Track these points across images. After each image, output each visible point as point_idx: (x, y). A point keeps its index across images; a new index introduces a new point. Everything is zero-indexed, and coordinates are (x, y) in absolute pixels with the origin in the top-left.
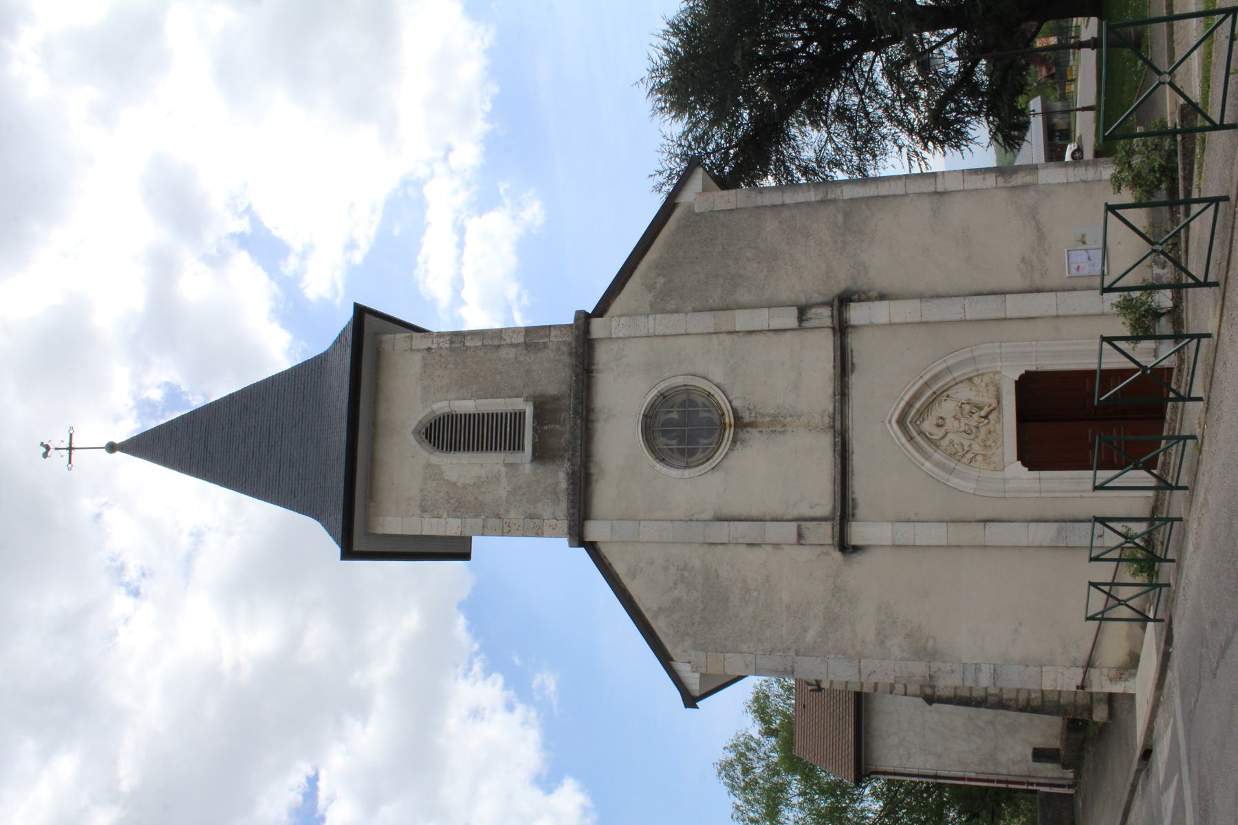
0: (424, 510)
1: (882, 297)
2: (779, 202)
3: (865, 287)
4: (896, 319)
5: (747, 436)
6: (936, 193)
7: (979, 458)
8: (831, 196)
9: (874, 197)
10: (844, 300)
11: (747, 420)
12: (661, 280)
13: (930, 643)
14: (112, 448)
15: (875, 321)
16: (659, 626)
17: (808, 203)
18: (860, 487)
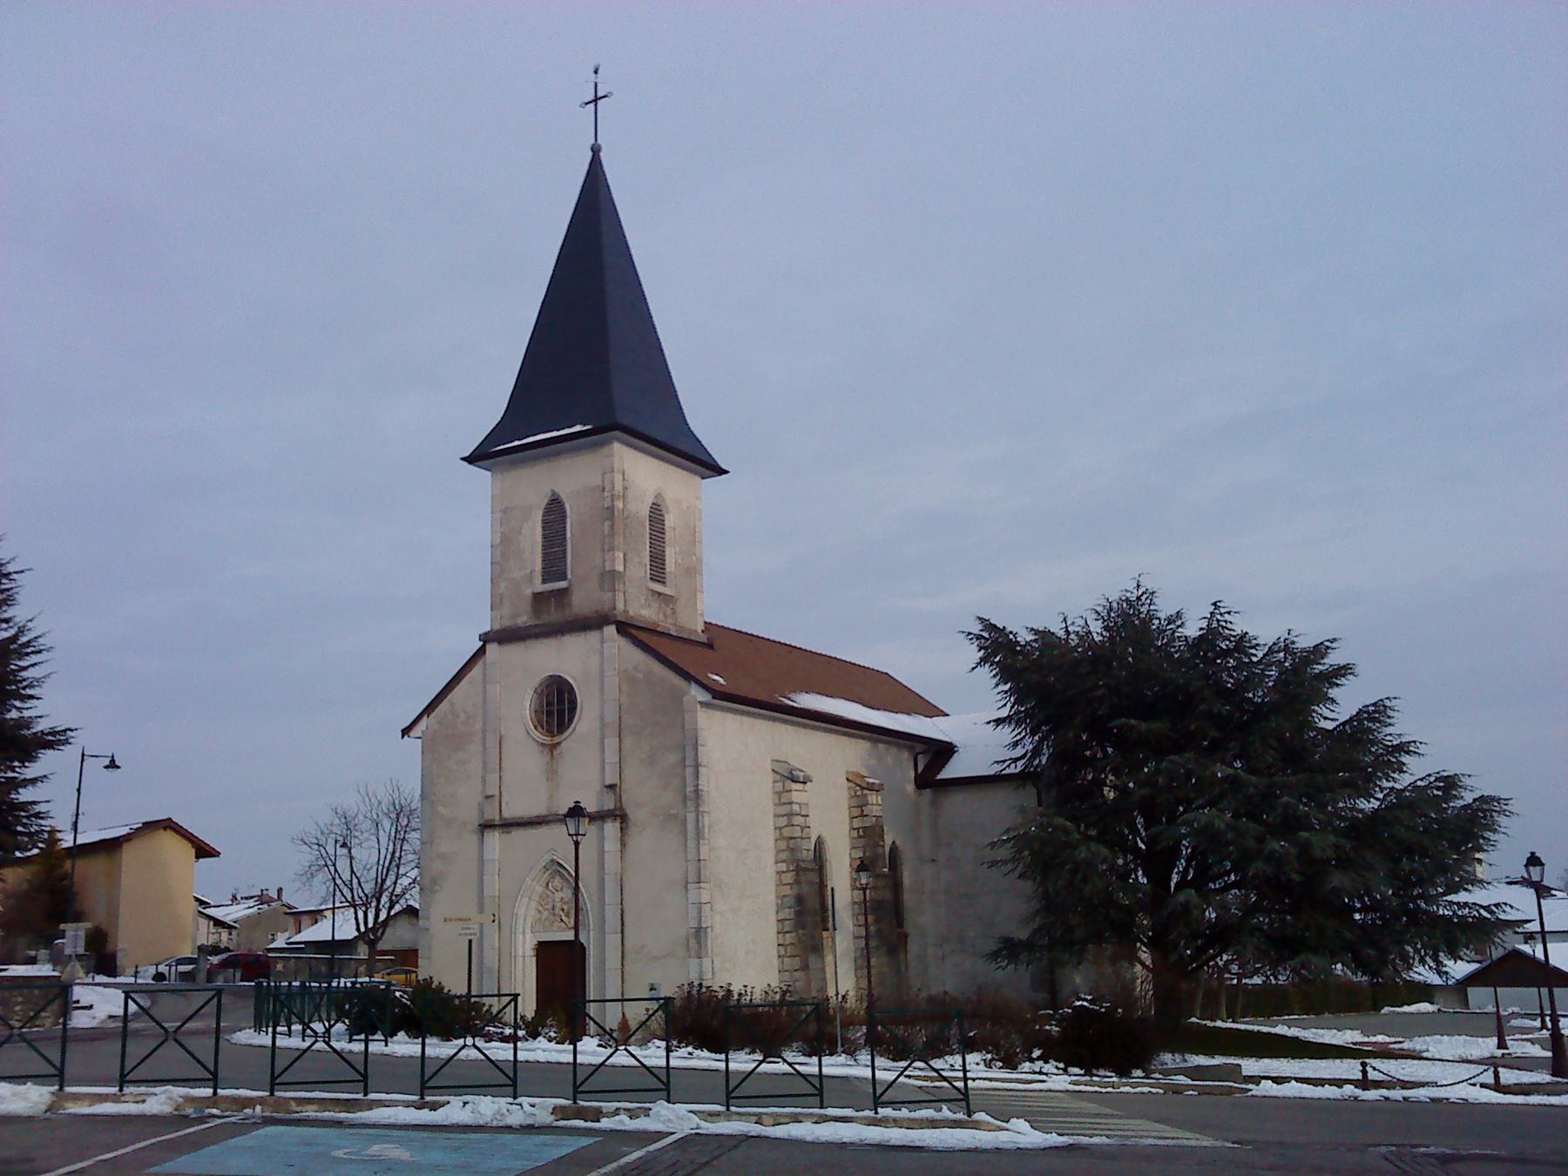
0: (504, 511)
1: (623, 844)
2: (687, 763)
3: (630, 832)
4: (606, 856)
5: (545, 753)
6: (687, 883)
7: (539, 916)
8: (689, 803)
9: (686, 836)
10: (619, 815)
11: (555, 752)
12: (641, 676)
13: (438, 888)
14: (596, 150)
15: (606, 840)
16: (444, 706)
17: (685, 786)
18: (519, 835)
